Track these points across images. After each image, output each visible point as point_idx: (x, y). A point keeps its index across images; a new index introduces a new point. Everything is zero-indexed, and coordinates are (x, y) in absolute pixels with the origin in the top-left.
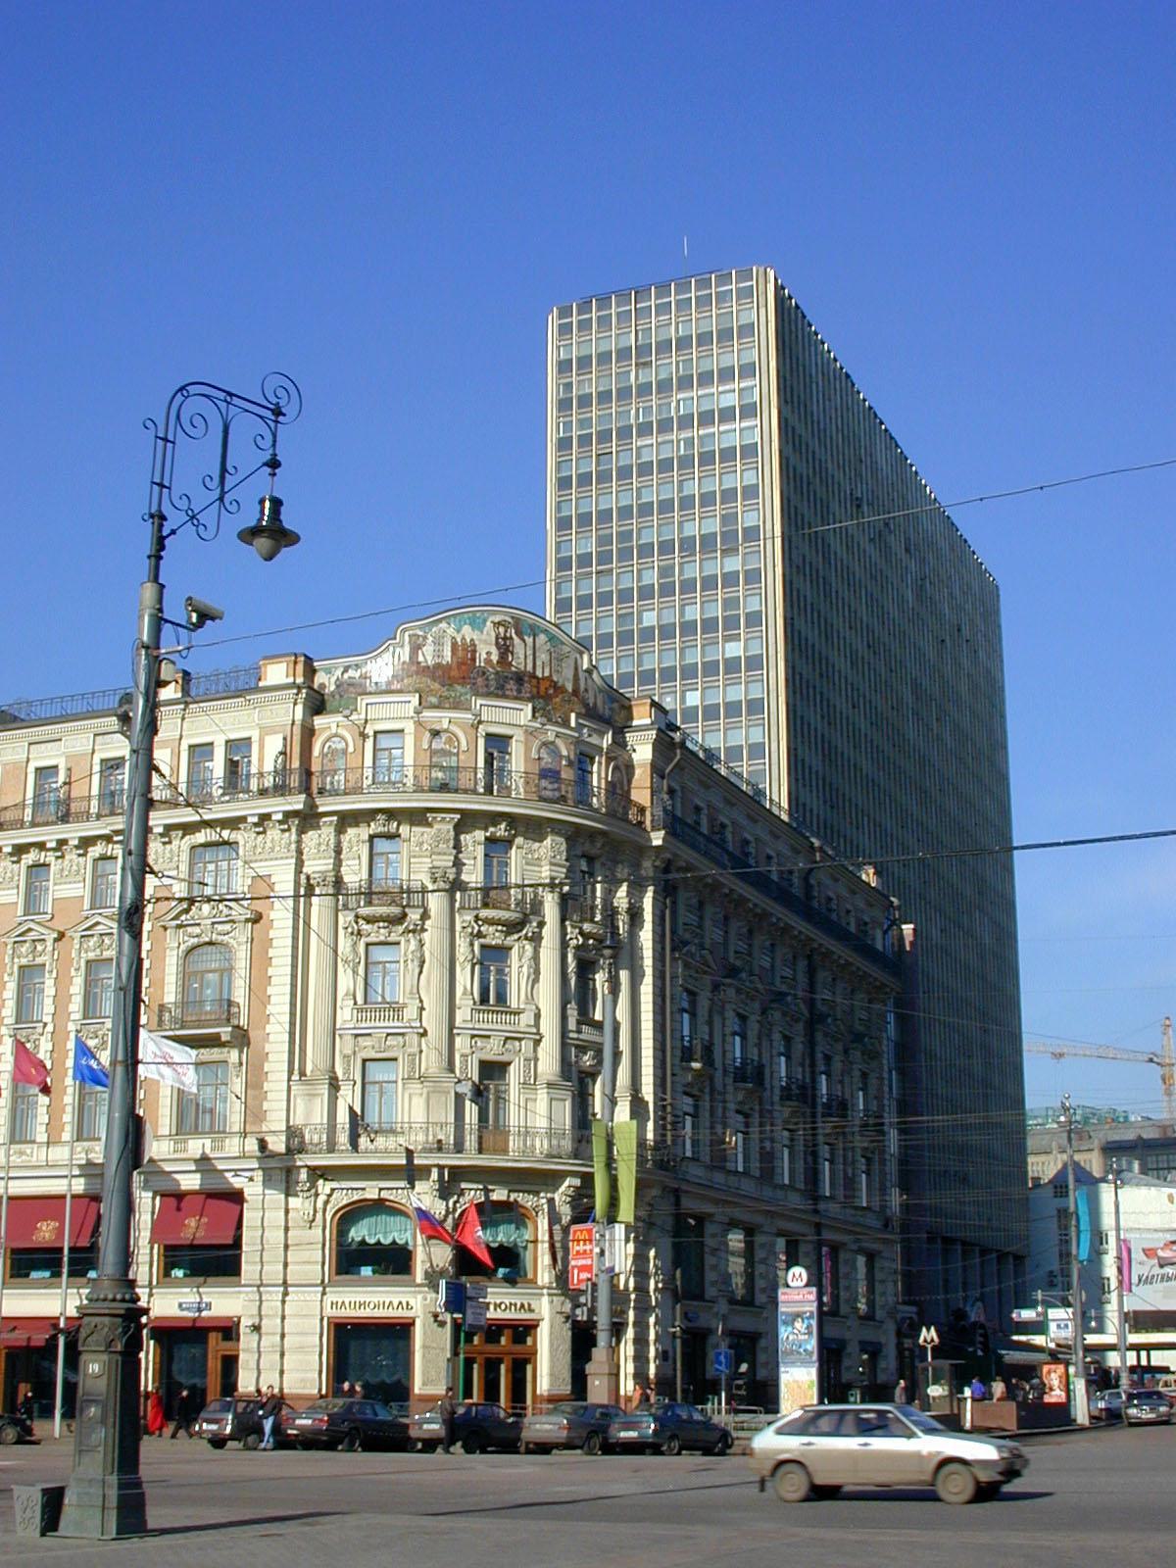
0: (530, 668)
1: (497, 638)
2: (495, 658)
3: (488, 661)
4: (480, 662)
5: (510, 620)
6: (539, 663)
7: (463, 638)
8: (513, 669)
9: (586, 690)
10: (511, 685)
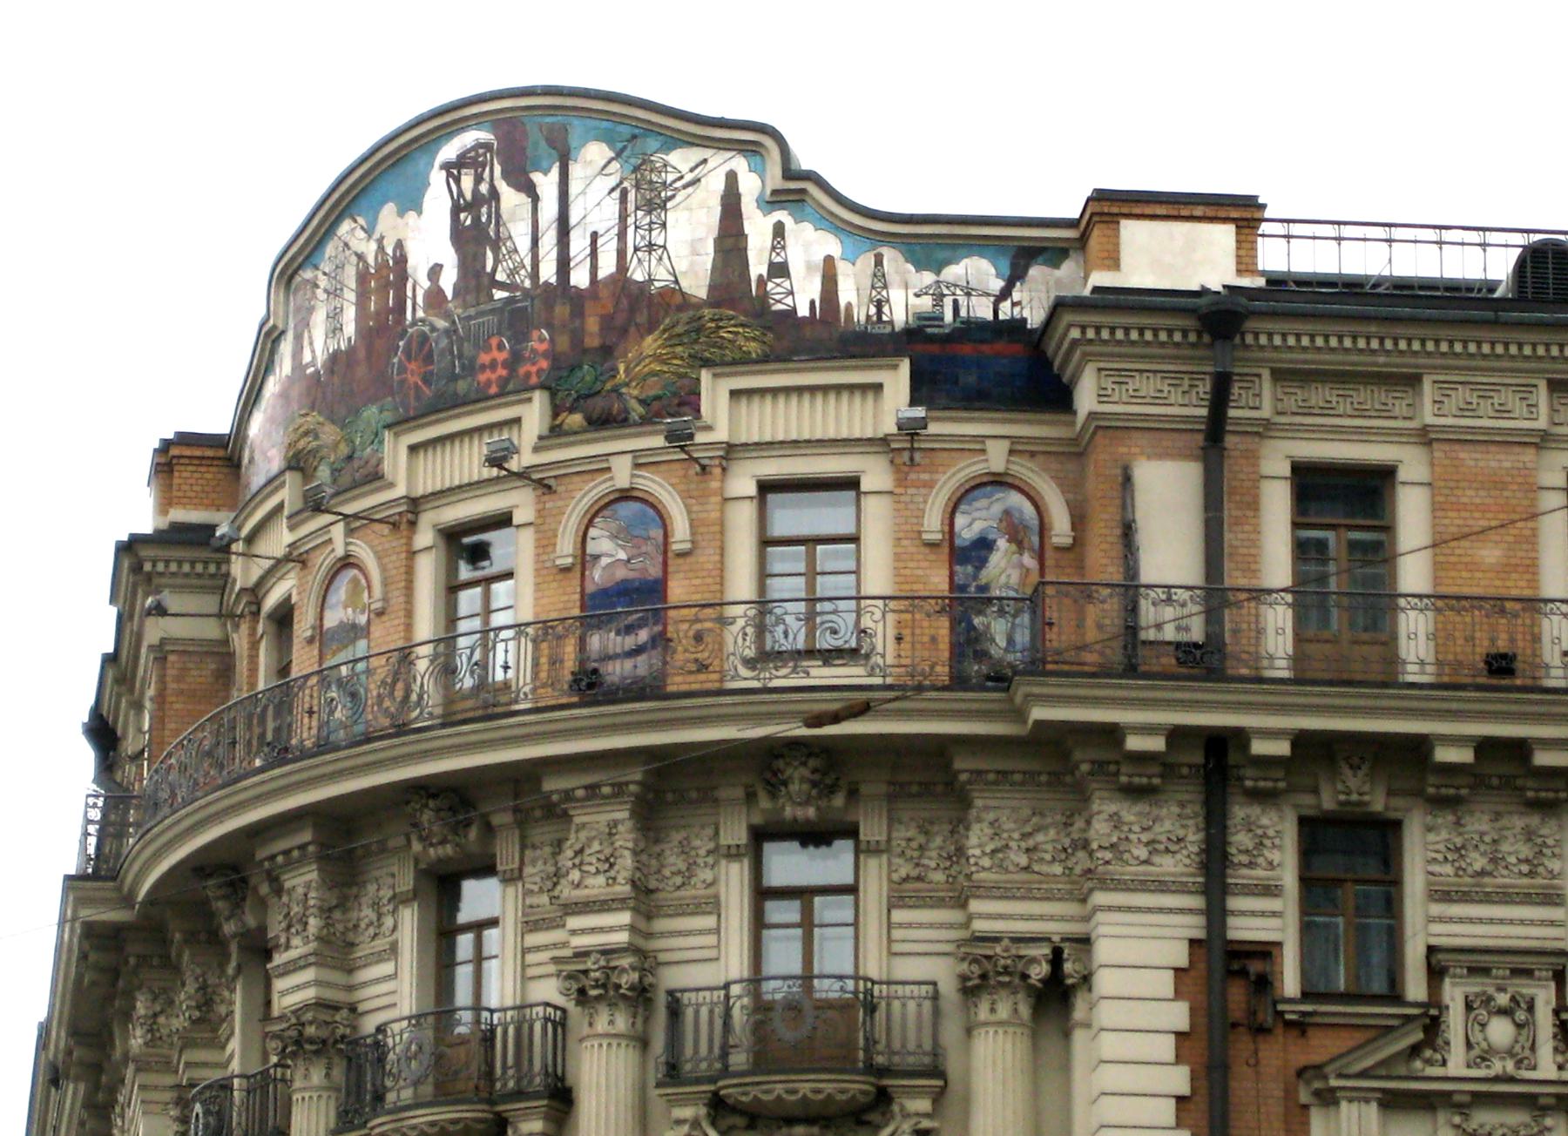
0: (548, 272)
1: (456, 210)
2: (448, 281)
3: (435, 297)
4: (416, 309)
5: (484, 136)
6: (579, 244)
7: (381, 248)
8: (499, 294)
9: (780, 270)
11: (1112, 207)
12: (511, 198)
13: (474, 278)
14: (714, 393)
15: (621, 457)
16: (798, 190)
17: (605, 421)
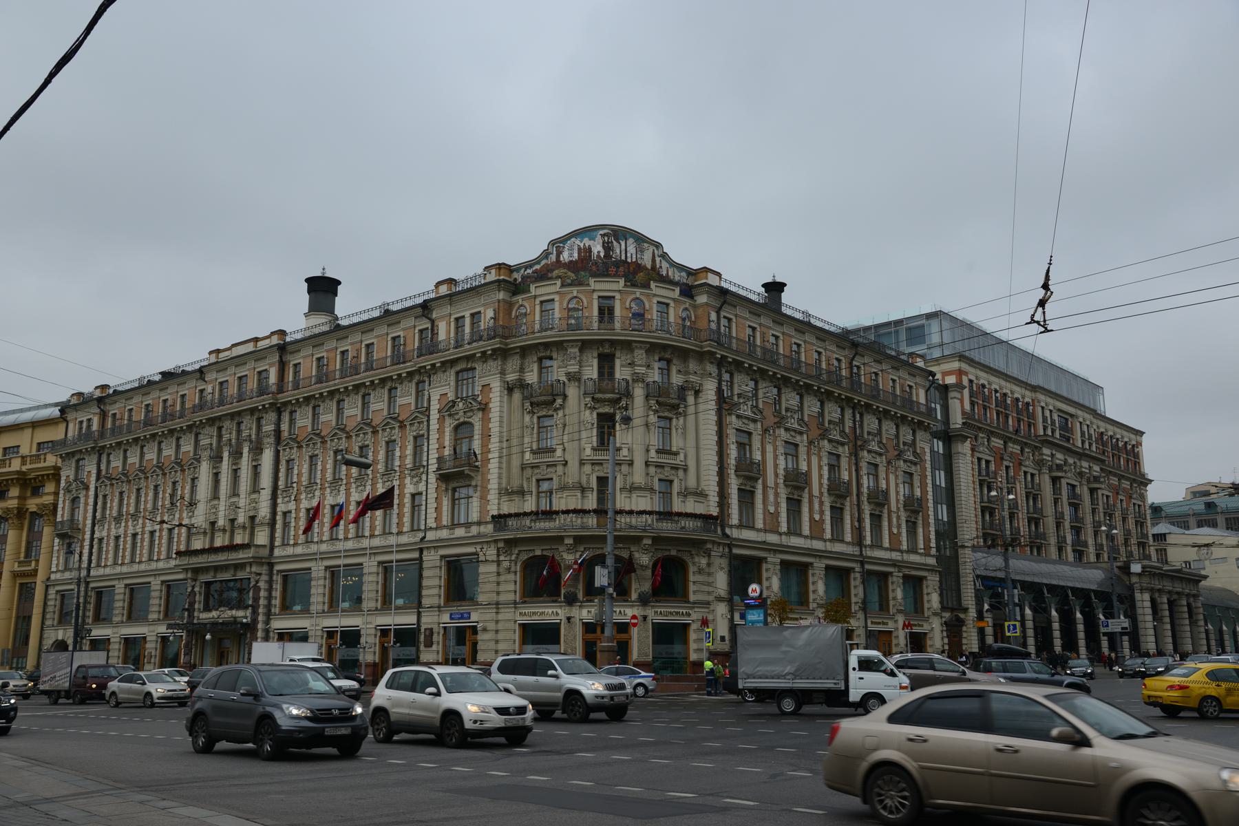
2: (602, 255)
3: (599, 256)
10: (613, 270)
11: (706, 270)
12: (615, 243)
13: (607, 256)
14: (653, 285)
15: (638, 292)
16: (664, 256)
17: (634, 285)
